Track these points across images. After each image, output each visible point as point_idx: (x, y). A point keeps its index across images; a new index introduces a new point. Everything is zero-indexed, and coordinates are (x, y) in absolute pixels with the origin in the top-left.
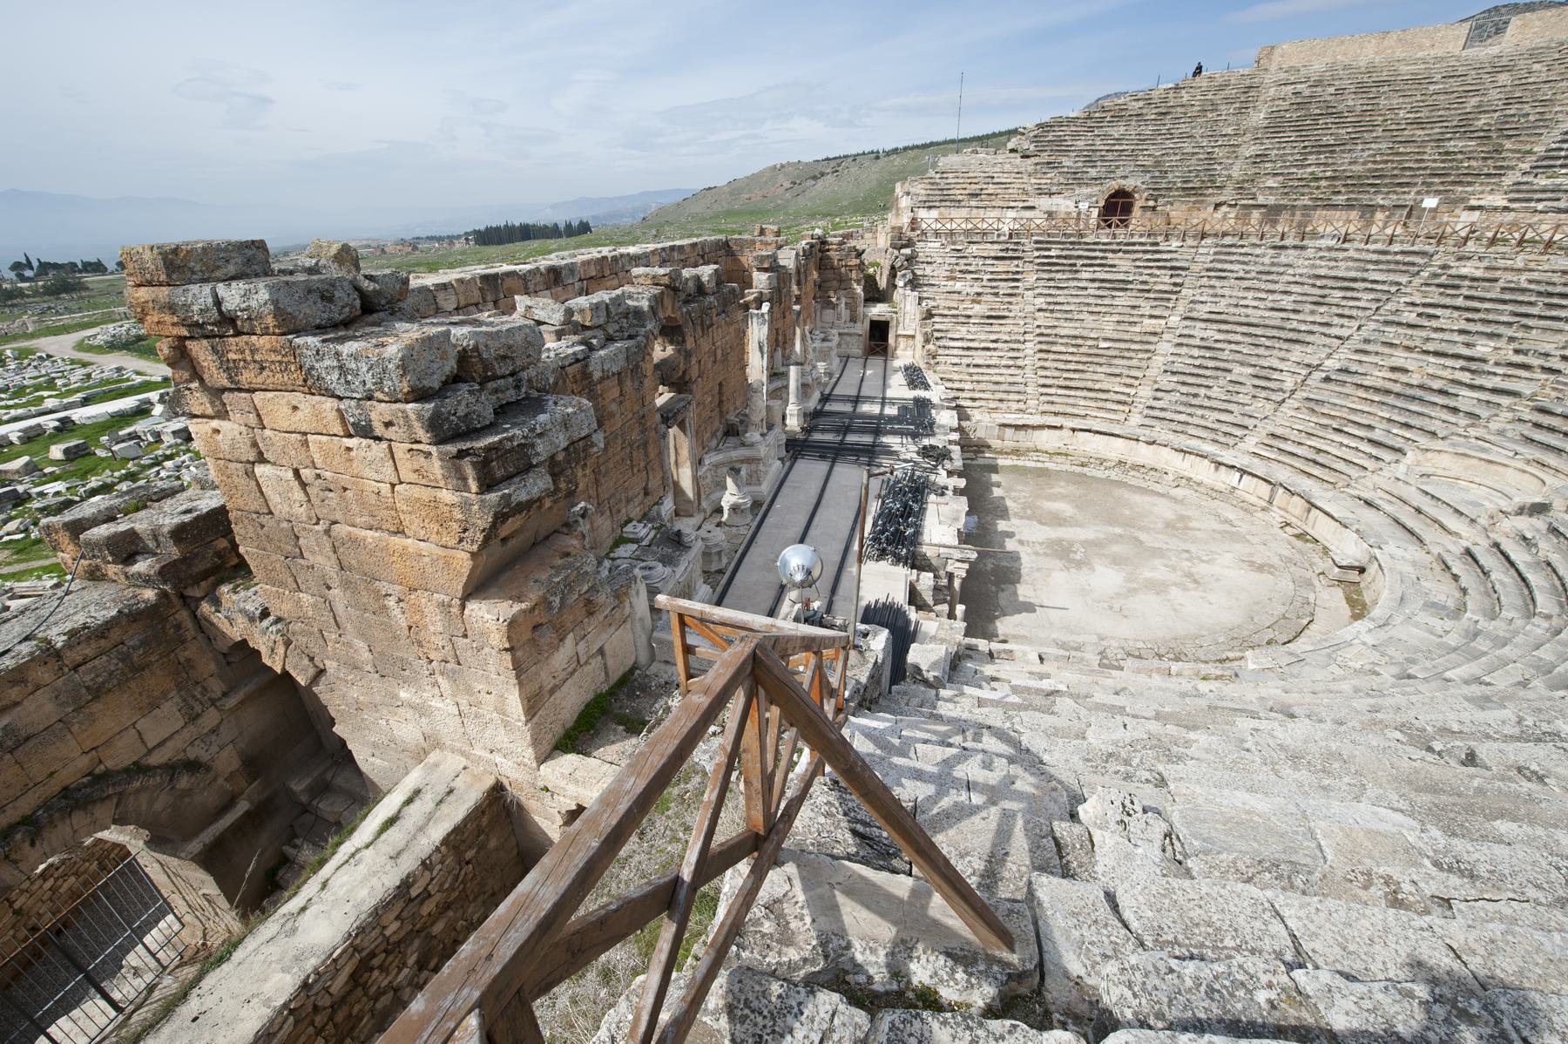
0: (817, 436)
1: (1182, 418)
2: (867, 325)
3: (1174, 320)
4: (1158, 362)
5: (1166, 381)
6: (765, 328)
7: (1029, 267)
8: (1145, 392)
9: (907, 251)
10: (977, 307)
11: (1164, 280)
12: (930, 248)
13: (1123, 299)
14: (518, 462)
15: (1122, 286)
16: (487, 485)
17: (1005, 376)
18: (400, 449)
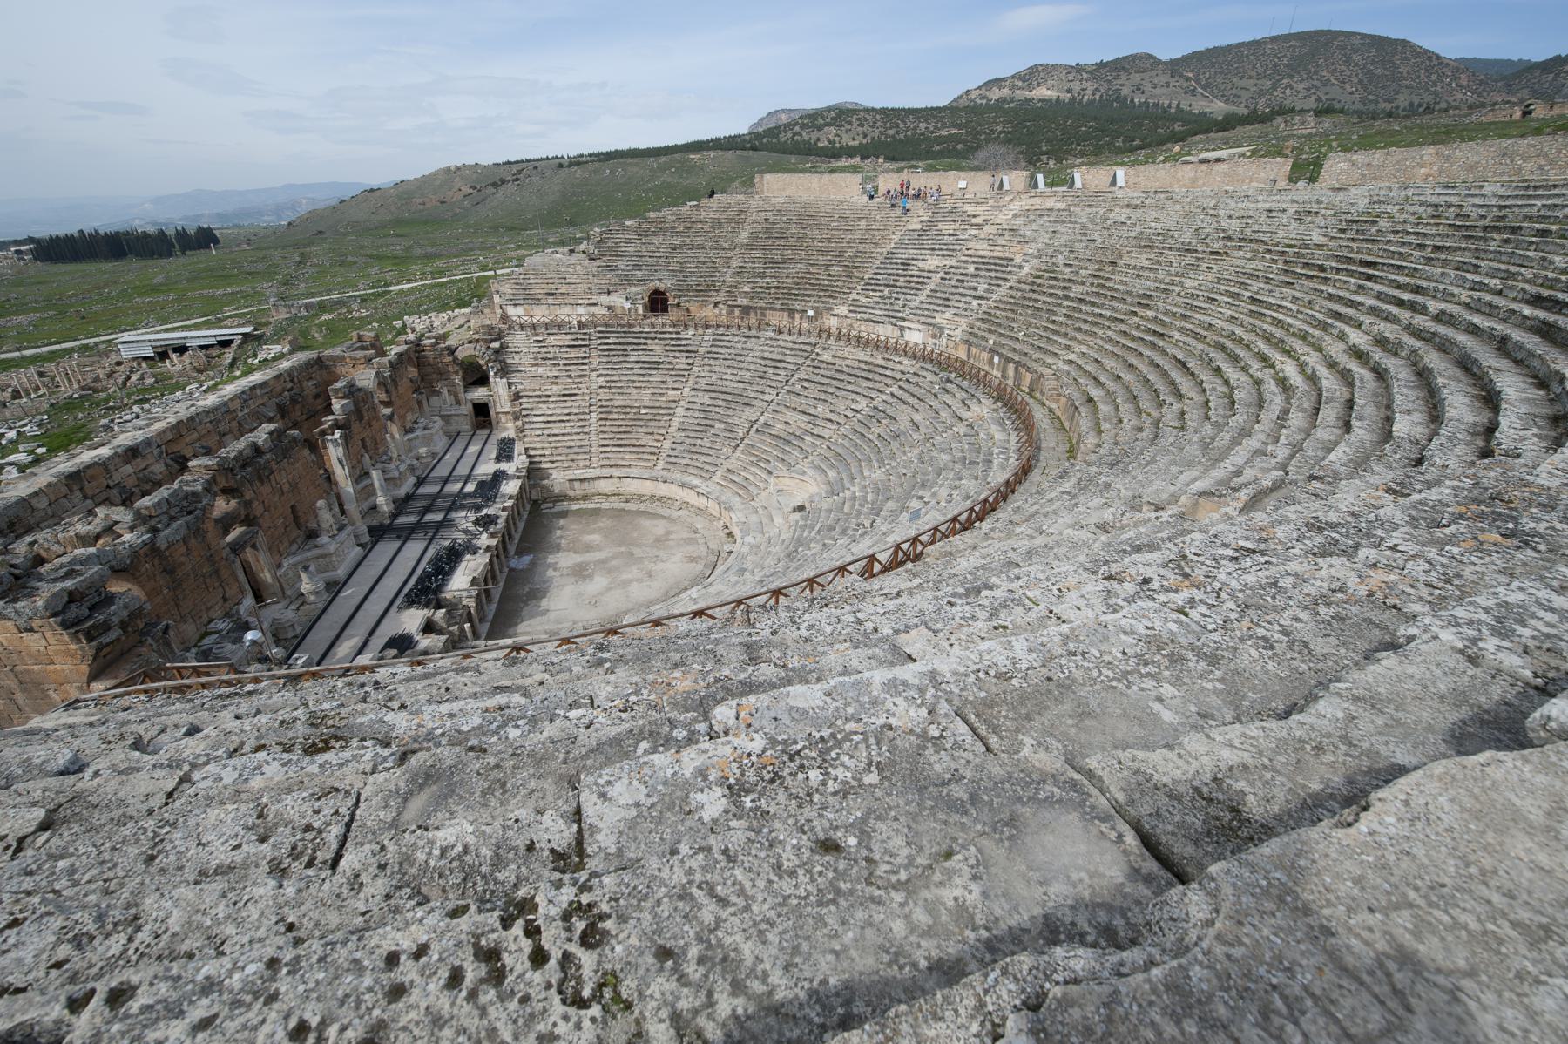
0: (402, 520)
1: (685, 461)
2: (470, 406)
3: (687, 390)
4: (676, 422)
5: (680, 436)
6: (341, 449)
7: (594, 353)
8: (667, 444)
9: (496, 345)
10: (555, 387)
11: (681, 362)
12: (518, 339)
13: (656, 377)
14: (106, 627)
15: (655, 366)
16: (90, 639)
17: (573, 441)
18: (48, 635)
